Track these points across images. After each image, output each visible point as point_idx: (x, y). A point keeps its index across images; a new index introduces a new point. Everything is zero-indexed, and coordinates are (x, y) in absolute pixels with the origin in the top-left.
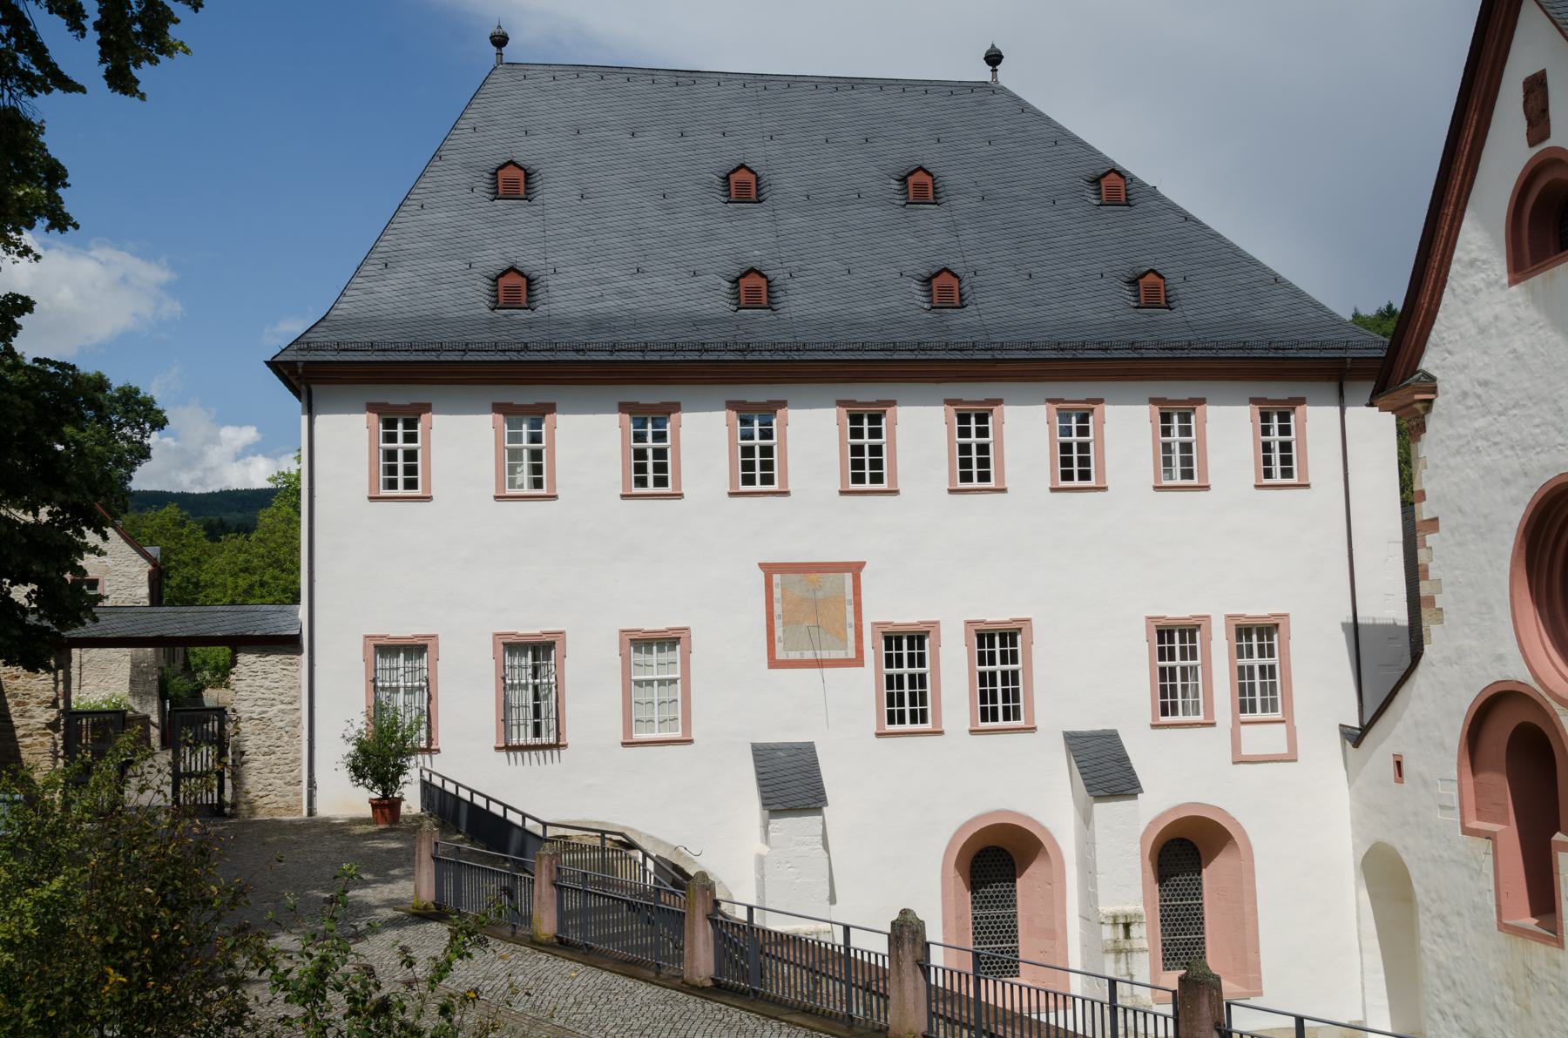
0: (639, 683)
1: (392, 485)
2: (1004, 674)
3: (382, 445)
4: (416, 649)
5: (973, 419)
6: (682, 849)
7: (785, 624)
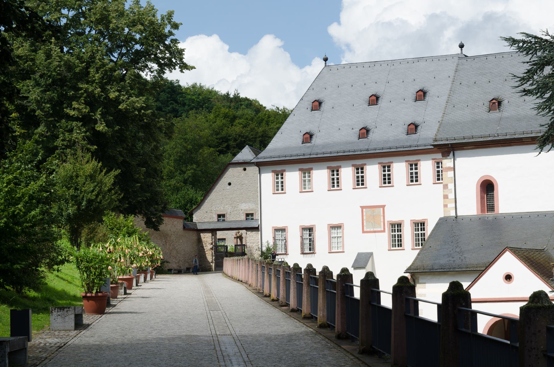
0: (333, 237)
1: (278, 190)
3: (276, 180)
4: (283, 230)
5: (414, 165)
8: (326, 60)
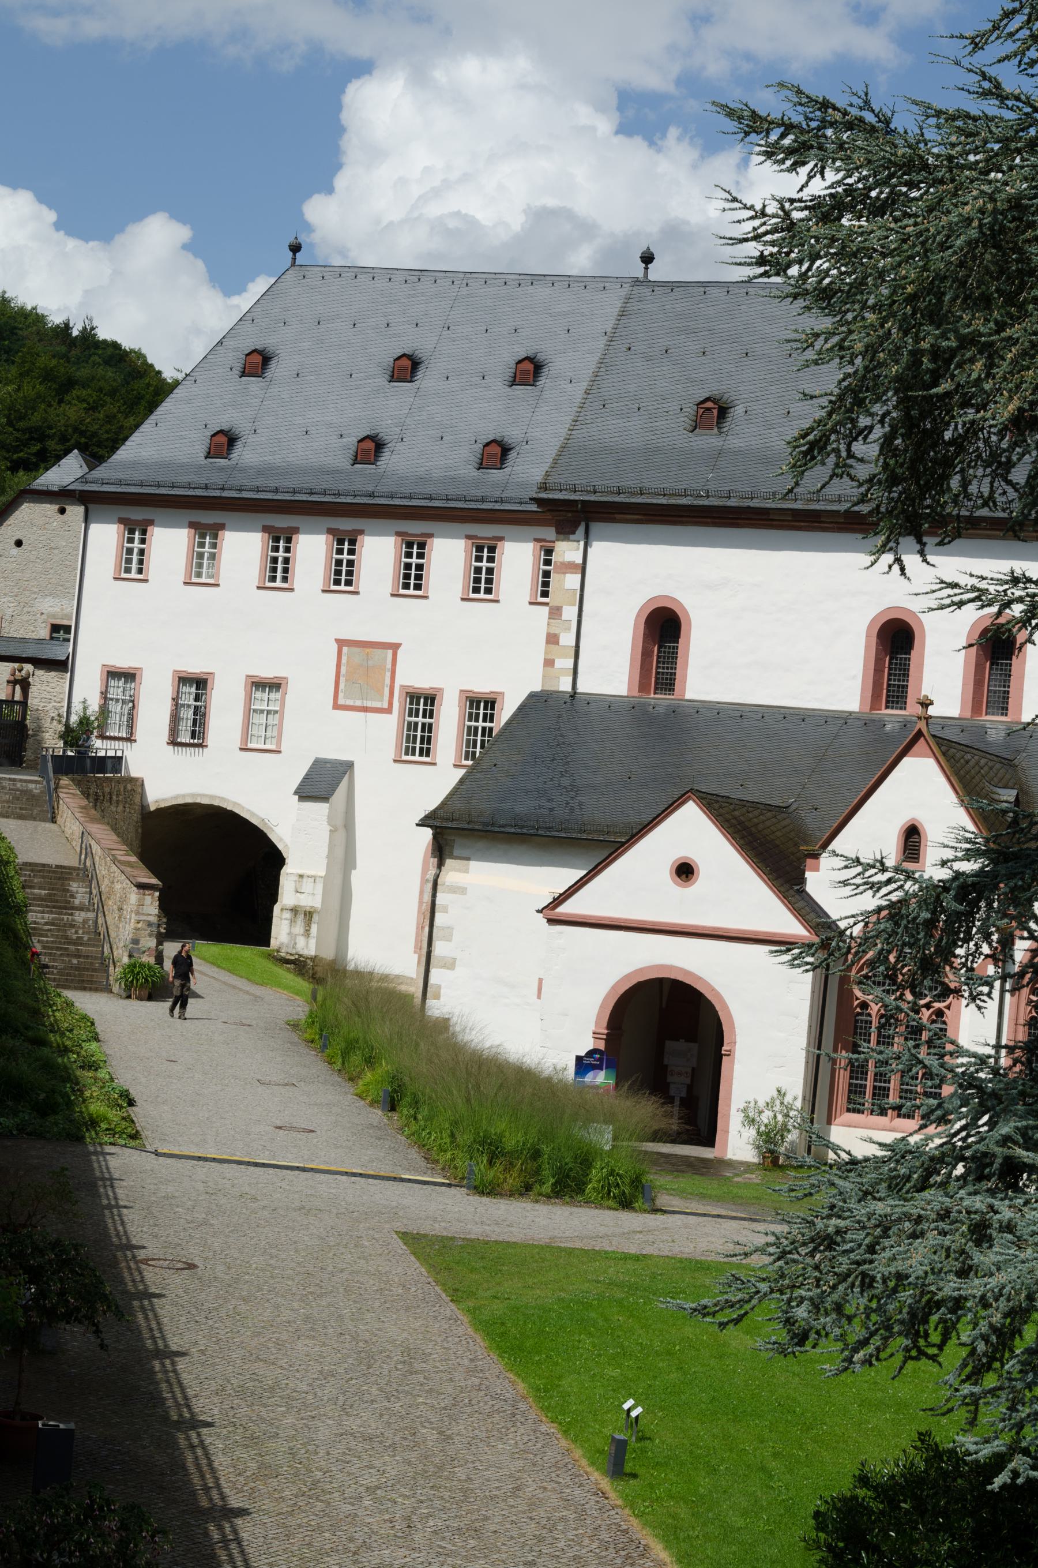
0: (255, 711)
2: (484, 729)
3: (126, 545)
4: (129, 676)
5: (486, 550)
7: (346, 680)
8: (295, 248)
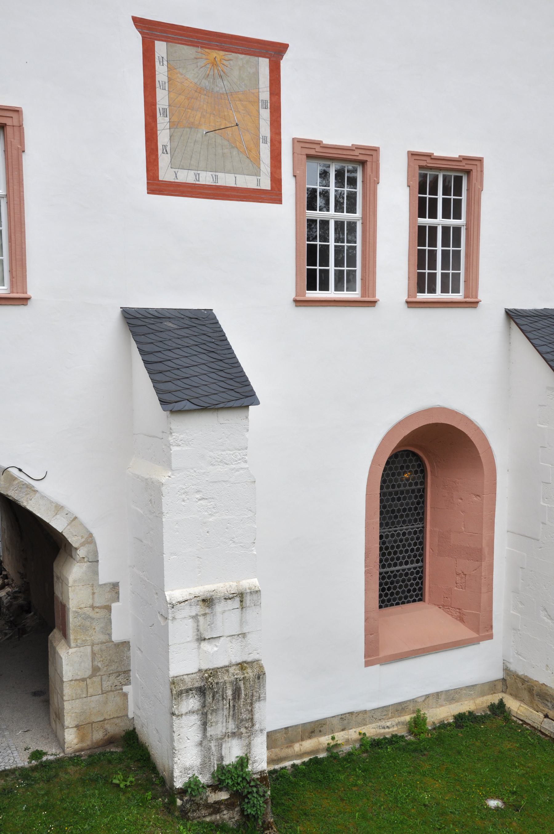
6: (15, 472)
7: (173, 125)
